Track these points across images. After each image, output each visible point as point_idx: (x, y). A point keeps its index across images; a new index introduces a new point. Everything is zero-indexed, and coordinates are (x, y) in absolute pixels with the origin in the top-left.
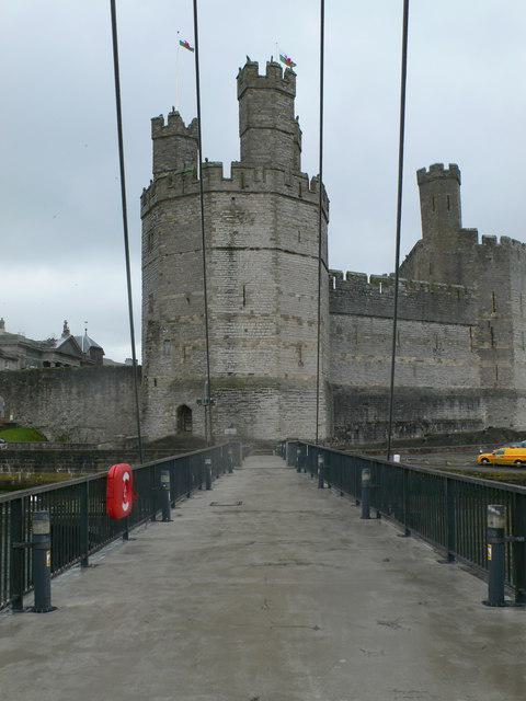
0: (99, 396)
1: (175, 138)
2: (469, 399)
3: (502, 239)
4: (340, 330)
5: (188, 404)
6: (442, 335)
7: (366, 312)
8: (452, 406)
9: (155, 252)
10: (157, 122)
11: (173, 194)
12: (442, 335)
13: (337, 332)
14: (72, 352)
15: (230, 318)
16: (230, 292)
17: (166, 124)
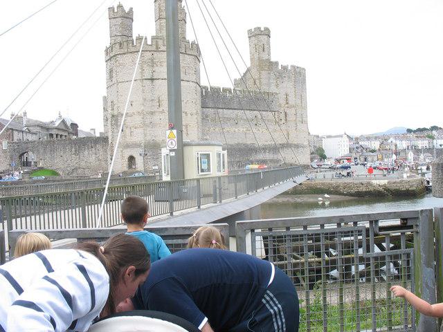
0: (86, 152)
1: (122, 18)
2: (275, 149)
3: (292, 66)
4: (207, 116)
5: (134, 155)
6: (259, 116)
7: (220, 107)
8: (265, 152)
9: (114, 80)
10: (111, 9)
11: (122, 51)
12: (259, 116)
13: (205, 118)
14: (63, 127)
15: (152, 113)
16: (152, 100)
17: (116, 11)
